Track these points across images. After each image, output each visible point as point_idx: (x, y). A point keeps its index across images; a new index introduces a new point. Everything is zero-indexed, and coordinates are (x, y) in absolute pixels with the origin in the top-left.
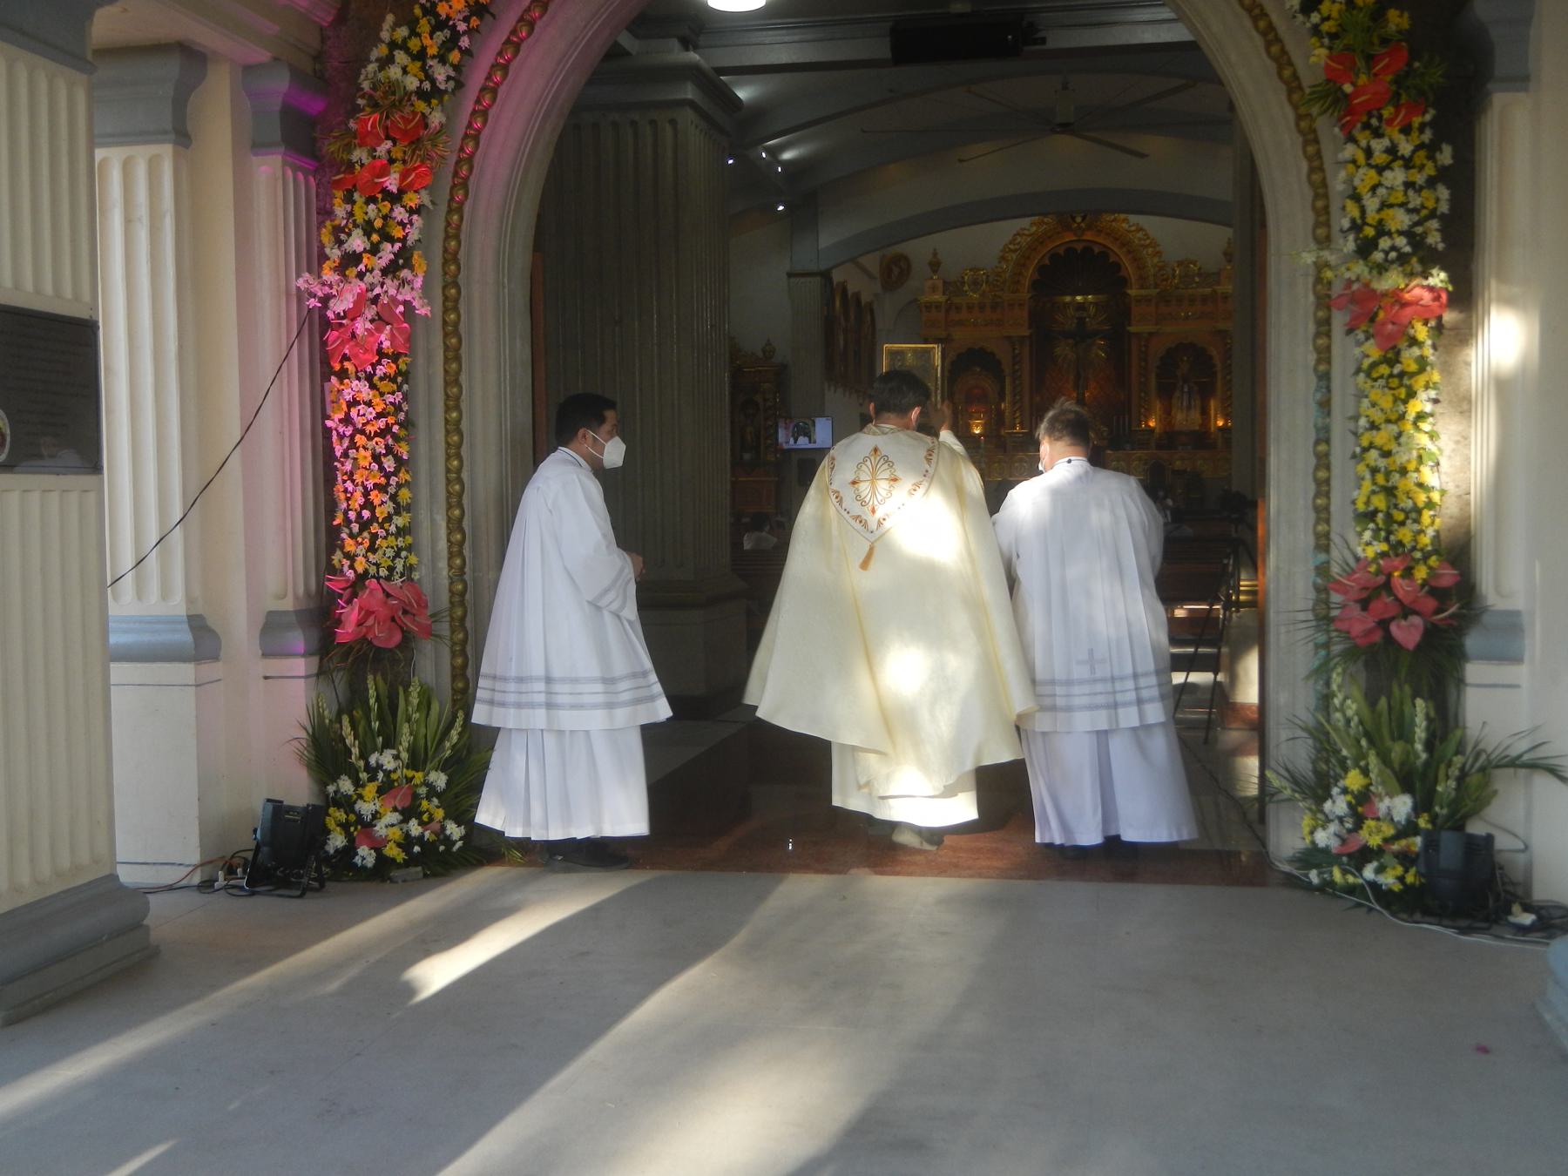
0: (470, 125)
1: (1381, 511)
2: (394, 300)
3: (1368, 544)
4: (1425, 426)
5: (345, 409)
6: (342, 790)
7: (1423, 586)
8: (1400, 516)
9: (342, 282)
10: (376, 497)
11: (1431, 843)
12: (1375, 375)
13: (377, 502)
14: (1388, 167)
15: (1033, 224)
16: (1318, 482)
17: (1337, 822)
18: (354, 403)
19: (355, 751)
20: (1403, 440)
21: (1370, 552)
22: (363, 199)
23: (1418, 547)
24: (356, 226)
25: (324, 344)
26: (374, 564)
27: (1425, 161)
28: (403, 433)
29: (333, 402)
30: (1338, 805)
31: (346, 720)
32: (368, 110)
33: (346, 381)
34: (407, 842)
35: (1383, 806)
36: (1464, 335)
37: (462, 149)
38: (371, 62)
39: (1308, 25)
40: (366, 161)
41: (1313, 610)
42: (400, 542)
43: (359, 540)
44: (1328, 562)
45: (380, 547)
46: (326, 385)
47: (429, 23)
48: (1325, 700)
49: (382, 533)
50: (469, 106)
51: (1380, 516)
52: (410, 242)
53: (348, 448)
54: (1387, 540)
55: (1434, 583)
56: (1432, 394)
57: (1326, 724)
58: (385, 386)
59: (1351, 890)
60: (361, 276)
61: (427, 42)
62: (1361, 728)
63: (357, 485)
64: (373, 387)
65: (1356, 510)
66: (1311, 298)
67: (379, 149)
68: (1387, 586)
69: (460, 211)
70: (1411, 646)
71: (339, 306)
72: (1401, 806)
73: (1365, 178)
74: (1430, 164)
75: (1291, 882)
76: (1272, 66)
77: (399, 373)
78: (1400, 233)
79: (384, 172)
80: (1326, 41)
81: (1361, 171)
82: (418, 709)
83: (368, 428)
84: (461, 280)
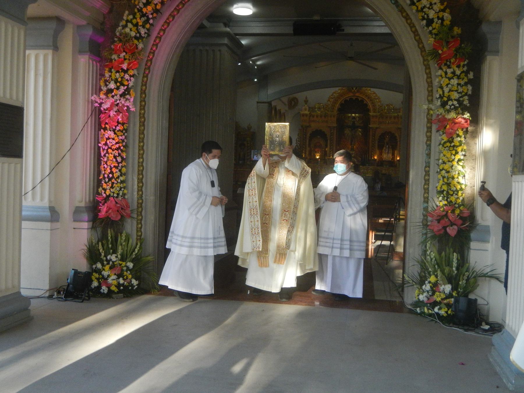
0: (152, 49)
1: (446, 191)
2: (123, 105)
4: (461, 163)
5: (105, 140)
6: (98, 267)
7: (458, 216)
8: (451, 193)
9: (106, 98)
10: (114, 170)
11: (457, 301)
12: (445, 146)
13: (114, 172)
14: (452, 78)
15: (339, 90)
16: (425, 180)
17: (426, 292)
18: (108, 139)
19: (103, 254)
20: (454, 167)
21: (441, 204)
22: (115, 71)
23: (457, 203)
24: (112, 80)
25: (99, 118)
26: (112, 192)
27: (464, 77)
28: (124, 149)
29: (101, 138)
30: (427, 287)
31: (100, 244)
32: (118, 42)
33: (106, 131)
34: (118, 285)
35: (441, 288)
36: (475, 134)
37: (149, 57)
38: (120, 26)
39: (428, 30)
40: (116, 59)
41: (422, 222)
42: (122, 185)
43: (108, 184)
44: (428, 207)
45: (115, 187)
46: (100, 132)
47: (140, 14)
48: (425, 251)
49: (115, 182)
50: (152, 42)
51: (445, 192)
52: (130, 86)
53: (106, 153)
54: (447, 200)
55: (461, 215)
56: (464, 153)
57: (425, 260)
58: (119, 133)
59: (430, 315)
60: (113, 97)
61: (139, 20)
62: (436, 262)
63: (108, 166)
64: (115, 133)
65: (437, 190)
66: (426, 119)
67: (121, 55)
68: (446, 215)
69: (147, 76)
70: (453, 236)
71: (105, 106)
72: (448, 288)
73: (444, 81)
74: (466, 78)
75: (411, 312)
76: (416, 43)
77: (124, 129)
78: (455, 100)
79: (122, 63)
80: (434, 36)
82: (125, 241)
83: (113, 147)
84: (146, 99)
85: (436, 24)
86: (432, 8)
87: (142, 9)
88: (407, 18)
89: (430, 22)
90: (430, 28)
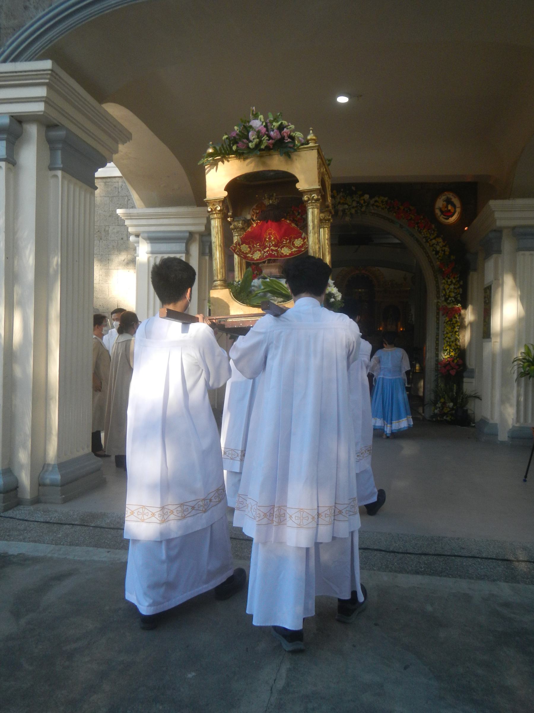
7: (456, 364)
21: (446, 357)
30: (439, 405)
35: (448, 404)
51: (448, 350)
54: (449, 355)
66: (436, 308)
72: (451, 404)
73: (448, 286)
78: (453, 297)
81: (446, 285)
85: (441, 254)
86: (438, 245)
89: (437, 253)
90: (438, 256)
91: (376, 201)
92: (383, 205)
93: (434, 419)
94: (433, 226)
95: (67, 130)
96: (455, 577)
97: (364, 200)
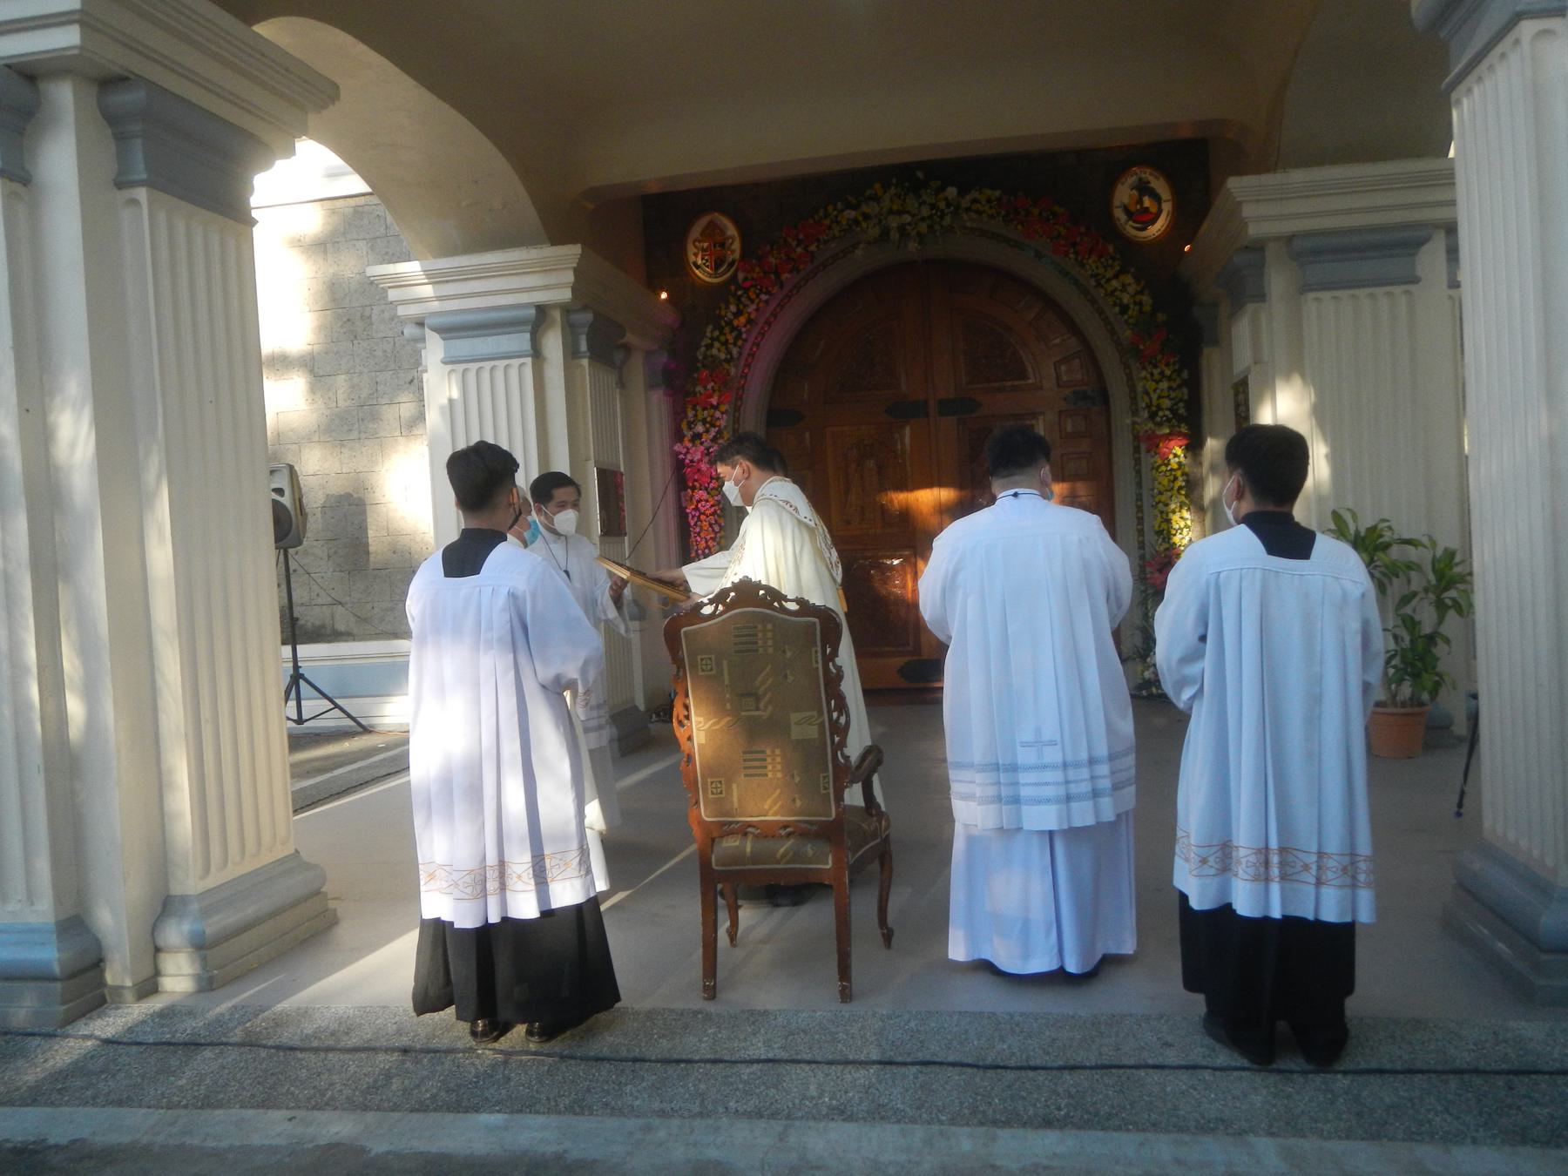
0: (743, 372)
3: (1161, 545)
9: (693, 446)
14: (1161, 381)
18: (699, 501)
21: (1162, 548)
46: (682, 493)
50: (743, 363)
51: (1165, 532)
52: (722, 427)
58: (713, 492)
60: (702, 443)
61: (729, 338)
64: (708, 493)
66: (1131, 437)
69: (739, 410)
73: (1151, 385)
74: (1178, 379)
78: (1167, 409)
79: (712, 397)
80: (1131, 327)
85: (1133, 311)
86: (1126, 291)
87: (731, 321)
88: (1093, 301)
90: (1126, 317)
91: (974, 201)
92: (991, 208)
93: (1144, 693)
94: (1111, 249)
95: (151, 85)
96: (1143, 1130)
97: (946, 199)
